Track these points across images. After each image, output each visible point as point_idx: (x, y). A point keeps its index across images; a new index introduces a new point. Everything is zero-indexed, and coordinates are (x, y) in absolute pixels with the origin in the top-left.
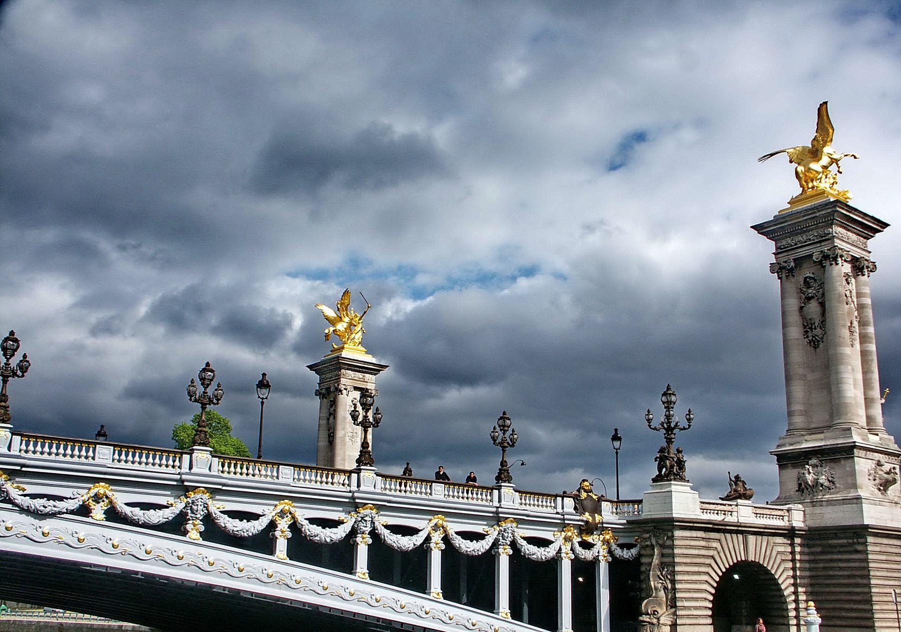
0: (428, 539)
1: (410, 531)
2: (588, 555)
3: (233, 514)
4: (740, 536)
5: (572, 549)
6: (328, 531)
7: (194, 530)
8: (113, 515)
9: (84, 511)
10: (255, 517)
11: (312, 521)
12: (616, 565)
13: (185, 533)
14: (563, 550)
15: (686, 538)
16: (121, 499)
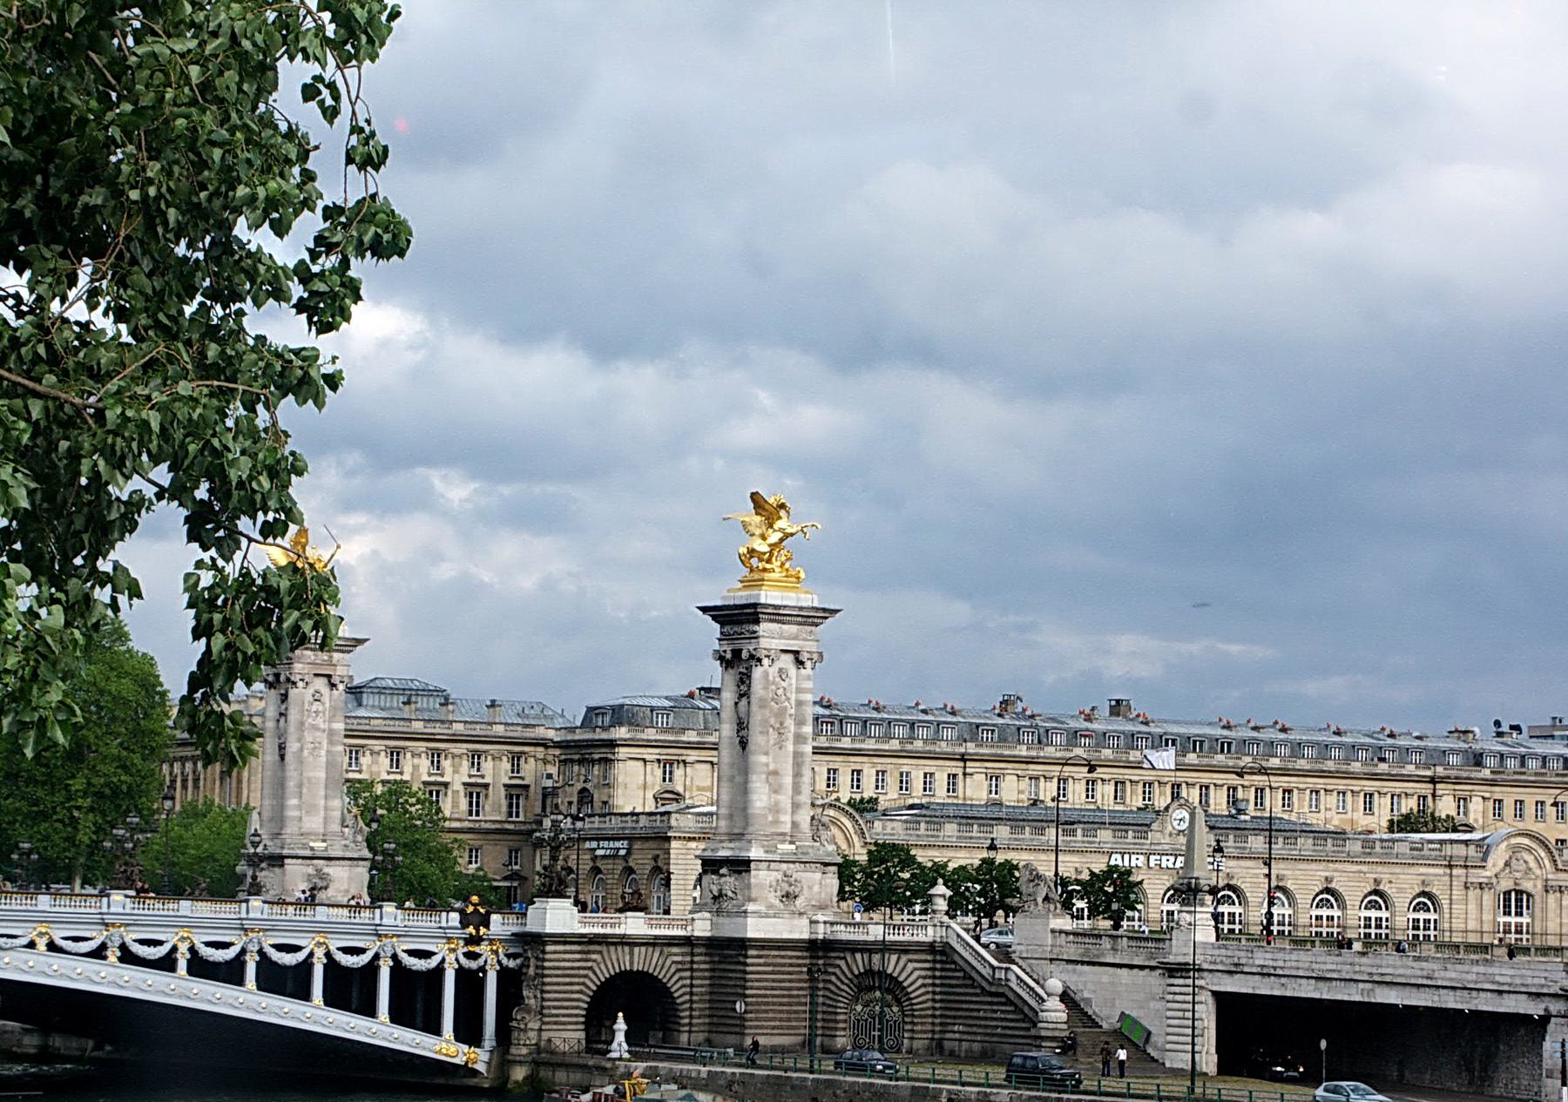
0: (311, 954)
1: (297, 949)
2: (473, 965)
3: (142, 942)
4: (627, 949)
5: (457, 960)
6: (220, 952)
7: (113, 955)
8: (52, 947)
9: (32, 945)
10: (160, 943)
11: (208, 944)
12: (503, 973)
13: (105, 958)
14: (447, 960)
15: (555, 952)
16: (57, 935)
